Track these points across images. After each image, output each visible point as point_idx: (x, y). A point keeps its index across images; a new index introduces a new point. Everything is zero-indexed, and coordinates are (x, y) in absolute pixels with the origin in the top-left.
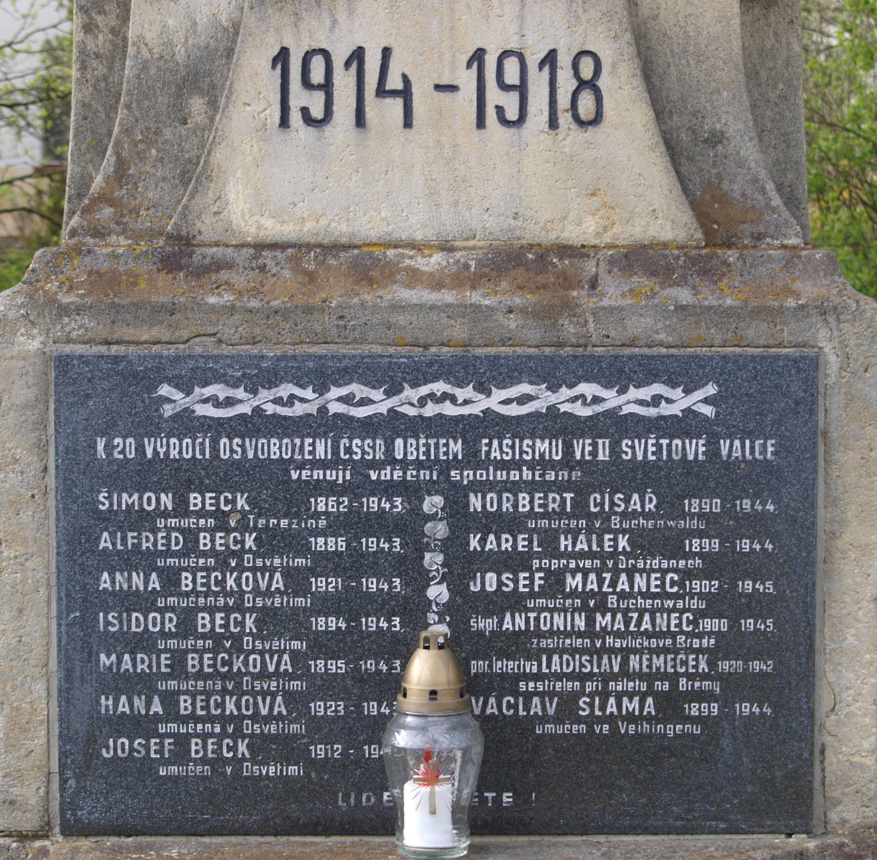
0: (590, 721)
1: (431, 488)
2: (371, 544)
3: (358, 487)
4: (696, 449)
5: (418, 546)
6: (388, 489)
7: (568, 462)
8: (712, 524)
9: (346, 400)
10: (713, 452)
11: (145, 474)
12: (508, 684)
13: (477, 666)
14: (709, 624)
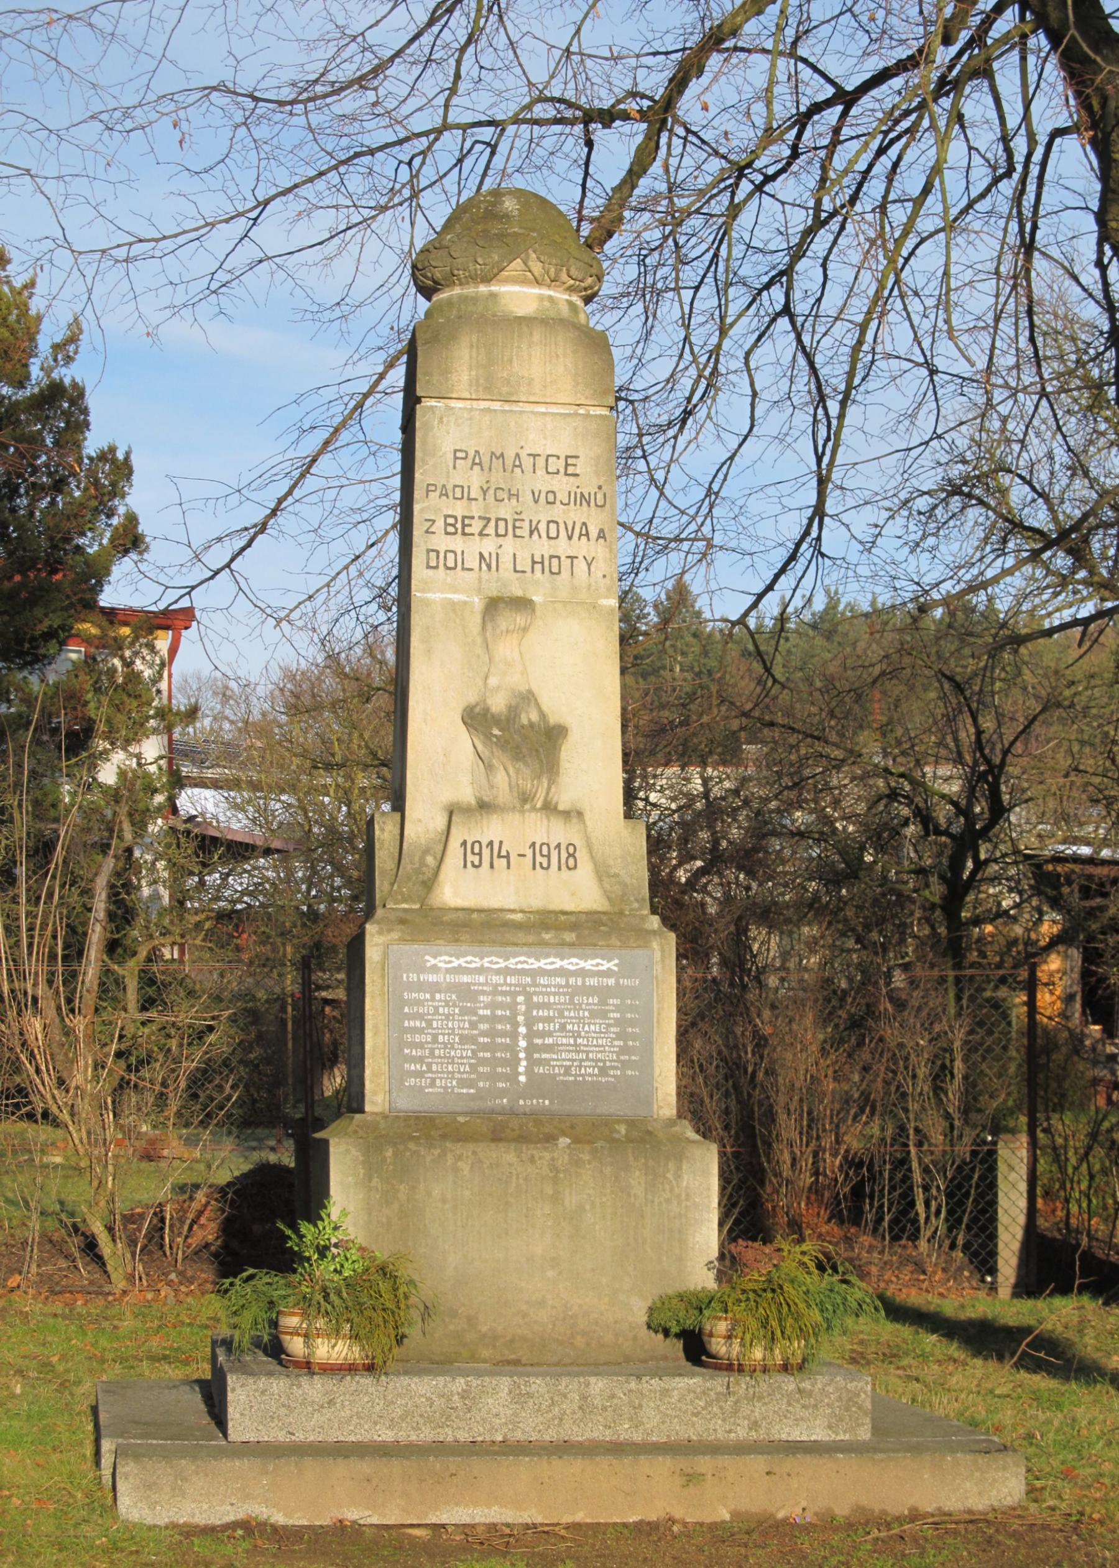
0: (576, 1075)
1: (519, 993)
2: (499, 1013)
3: (495, 992)
4: (611, 982)
5: (515, 1014)
6: (504, 993)
7: (567, 985)
8: (617, 1009)
9: (491, 962)
10: (617, 983)
11: (421, 987)
12: (547, 1062)
13: (536, 1056)
14: (616, 1043)
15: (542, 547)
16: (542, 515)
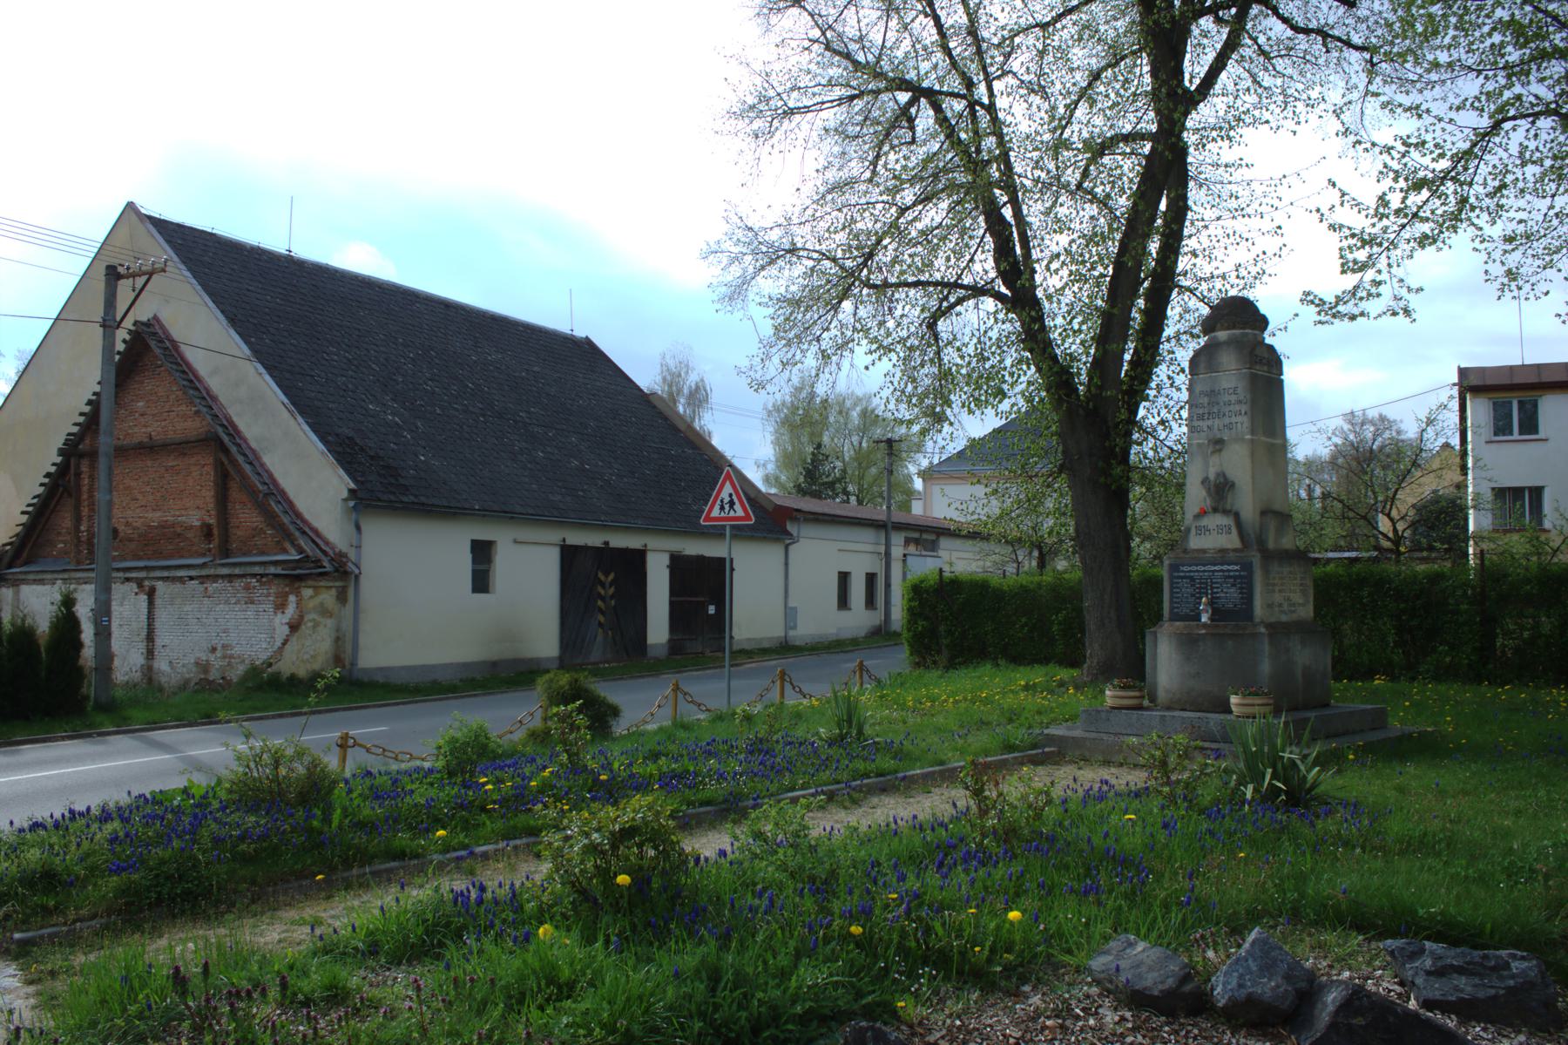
15: (1227, 420)
16: (1227, 409)
